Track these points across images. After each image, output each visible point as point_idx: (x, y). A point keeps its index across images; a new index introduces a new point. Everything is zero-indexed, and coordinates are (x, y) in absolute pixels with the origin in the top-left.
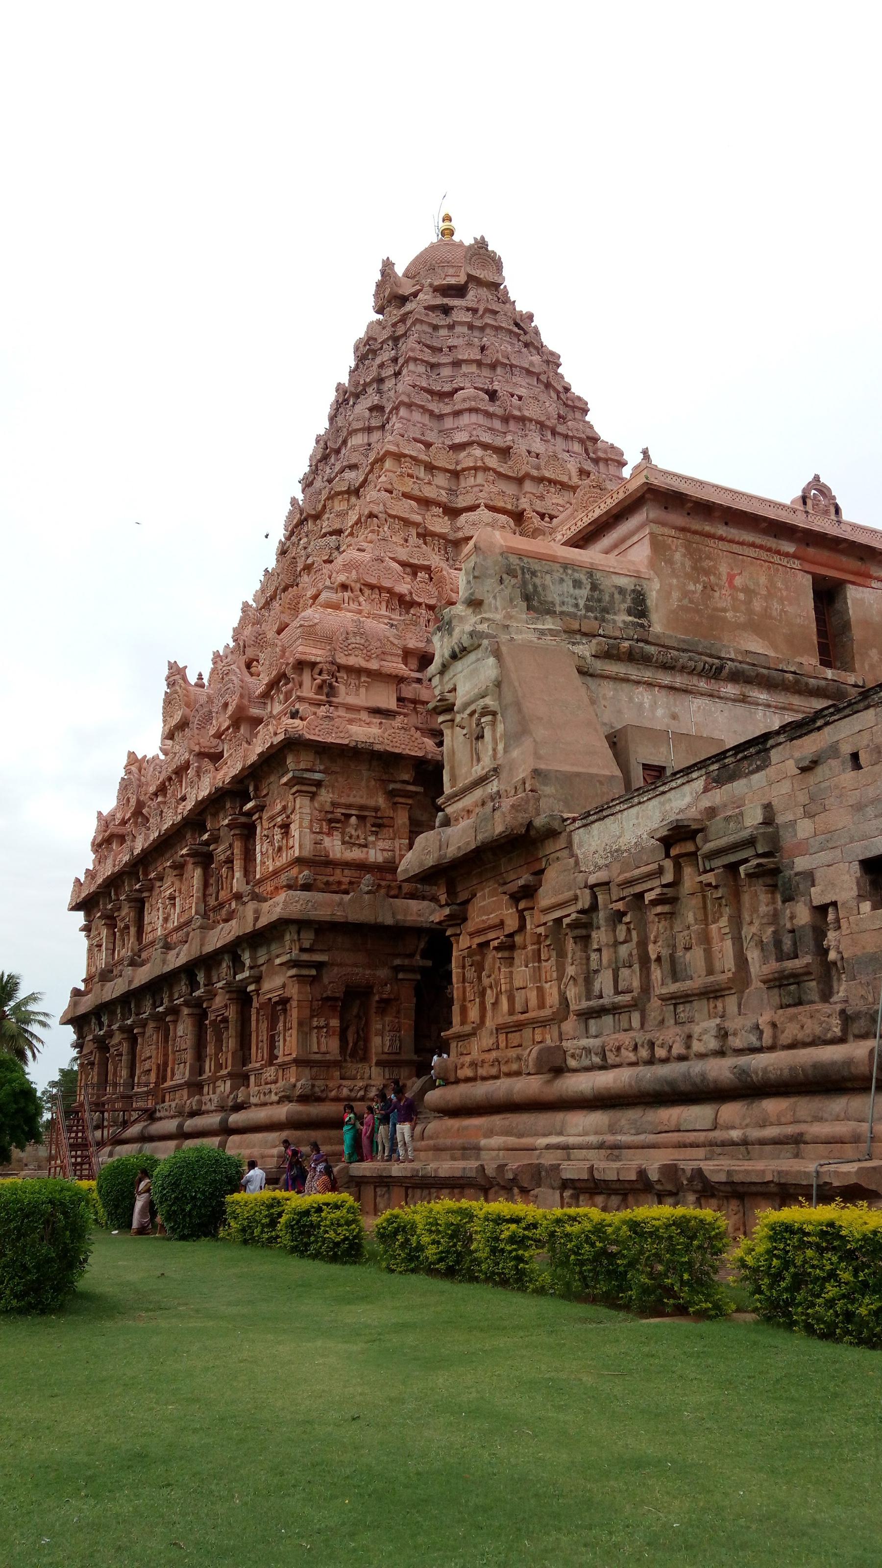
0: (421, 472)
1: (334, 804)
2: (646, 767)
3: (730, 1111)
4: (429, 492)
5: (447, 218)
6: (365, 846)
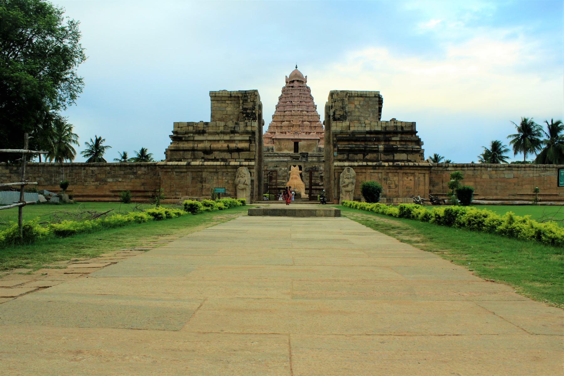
0: (279, 117)
4: (279, 120)
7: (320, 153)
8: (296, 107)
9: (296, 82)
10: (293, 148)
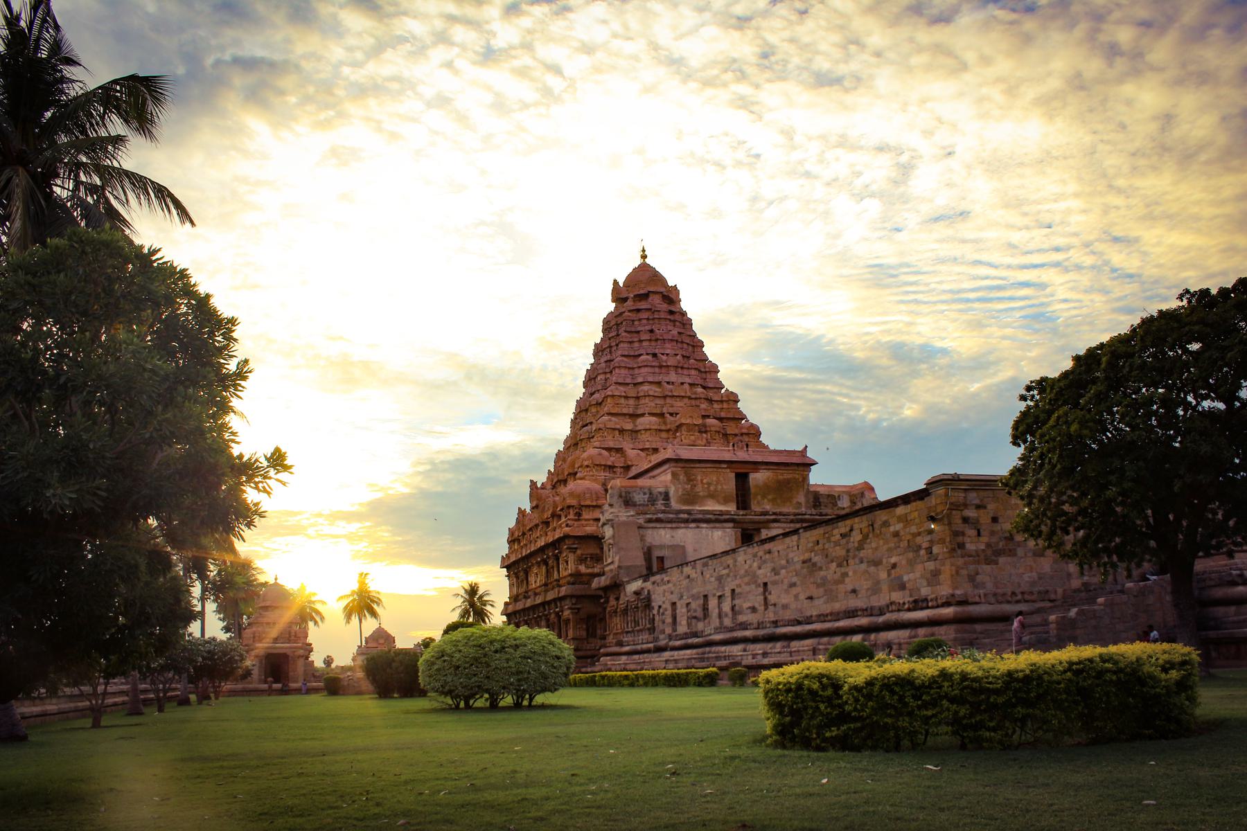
0: (622, 401)
1: (582, 555)
2: (658, 557)
3: (641, 656)
4: (625, 411)
5: (644, 251)
6: (593, 567)
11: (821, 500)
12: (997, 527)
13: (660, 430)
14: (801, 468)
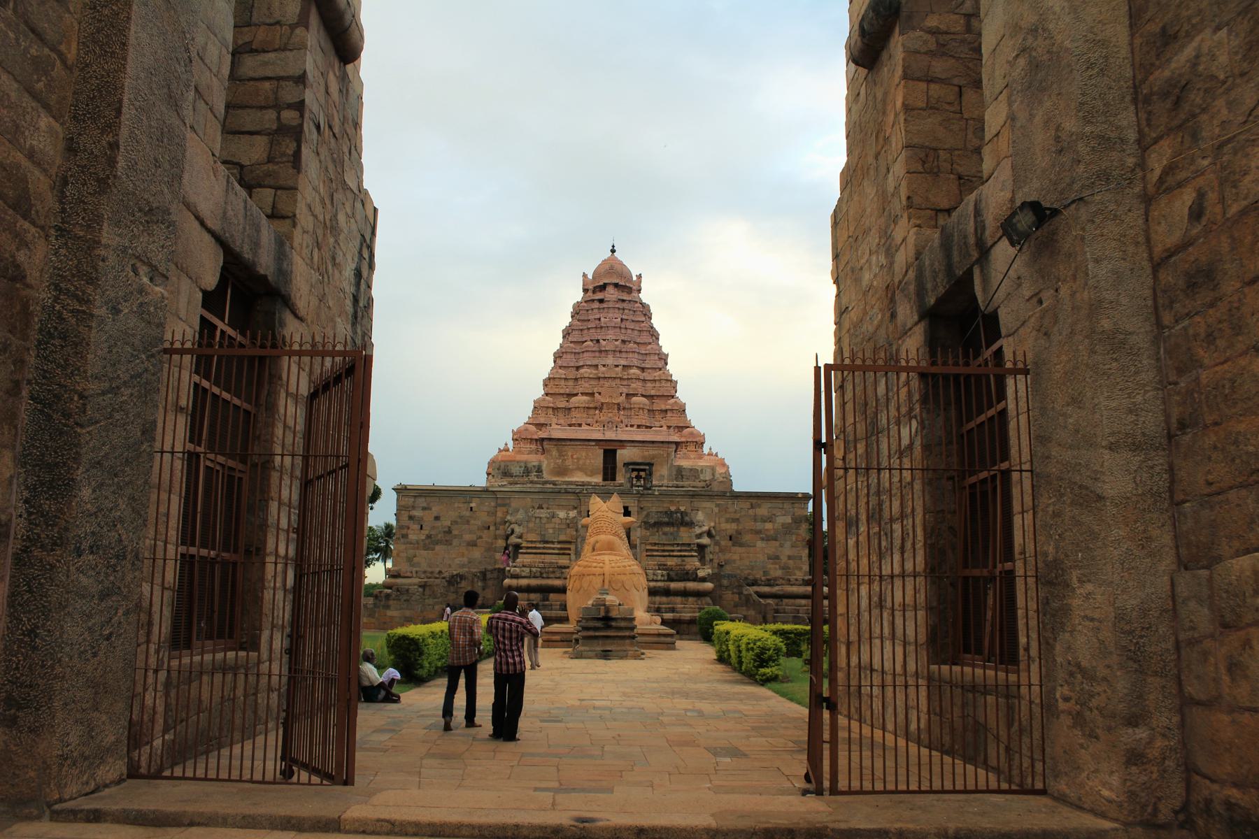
0: (563, 382)
4: (562, 391)
5: (613, 246)
7: (681, 483)
8: (610, 356)
9: (610, 289)
10: (602, 466)
11: (683, 473)
12: (438, 524)
13: (588, 408)
14: (666, 445)
